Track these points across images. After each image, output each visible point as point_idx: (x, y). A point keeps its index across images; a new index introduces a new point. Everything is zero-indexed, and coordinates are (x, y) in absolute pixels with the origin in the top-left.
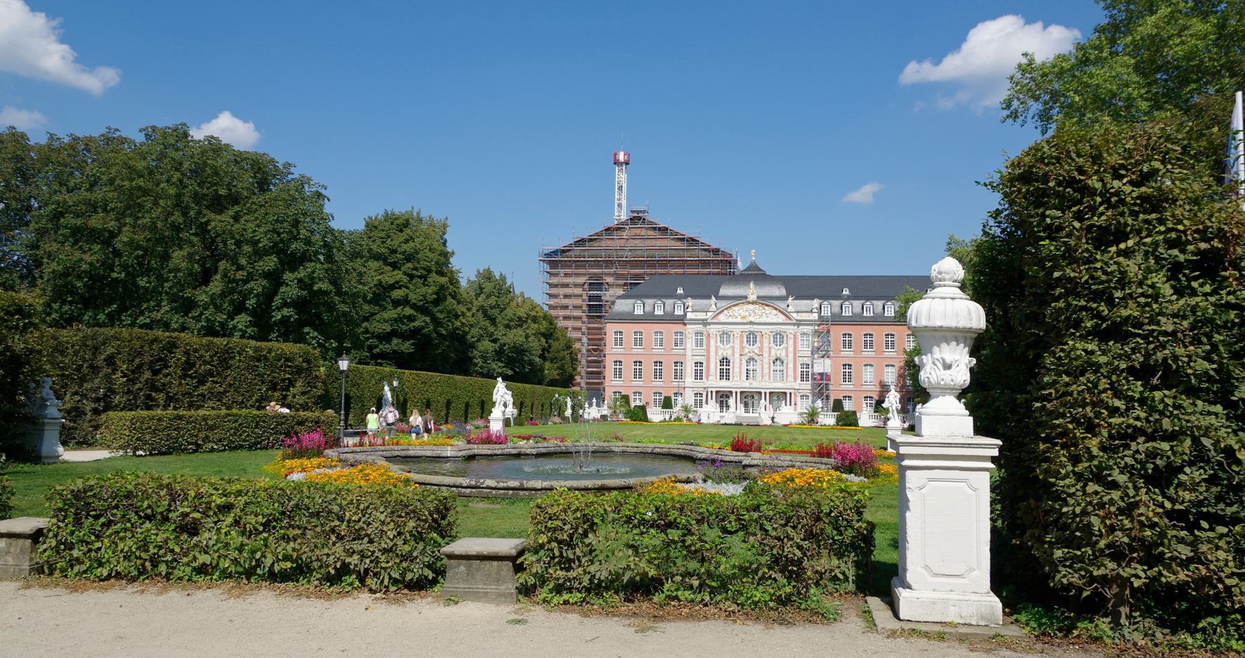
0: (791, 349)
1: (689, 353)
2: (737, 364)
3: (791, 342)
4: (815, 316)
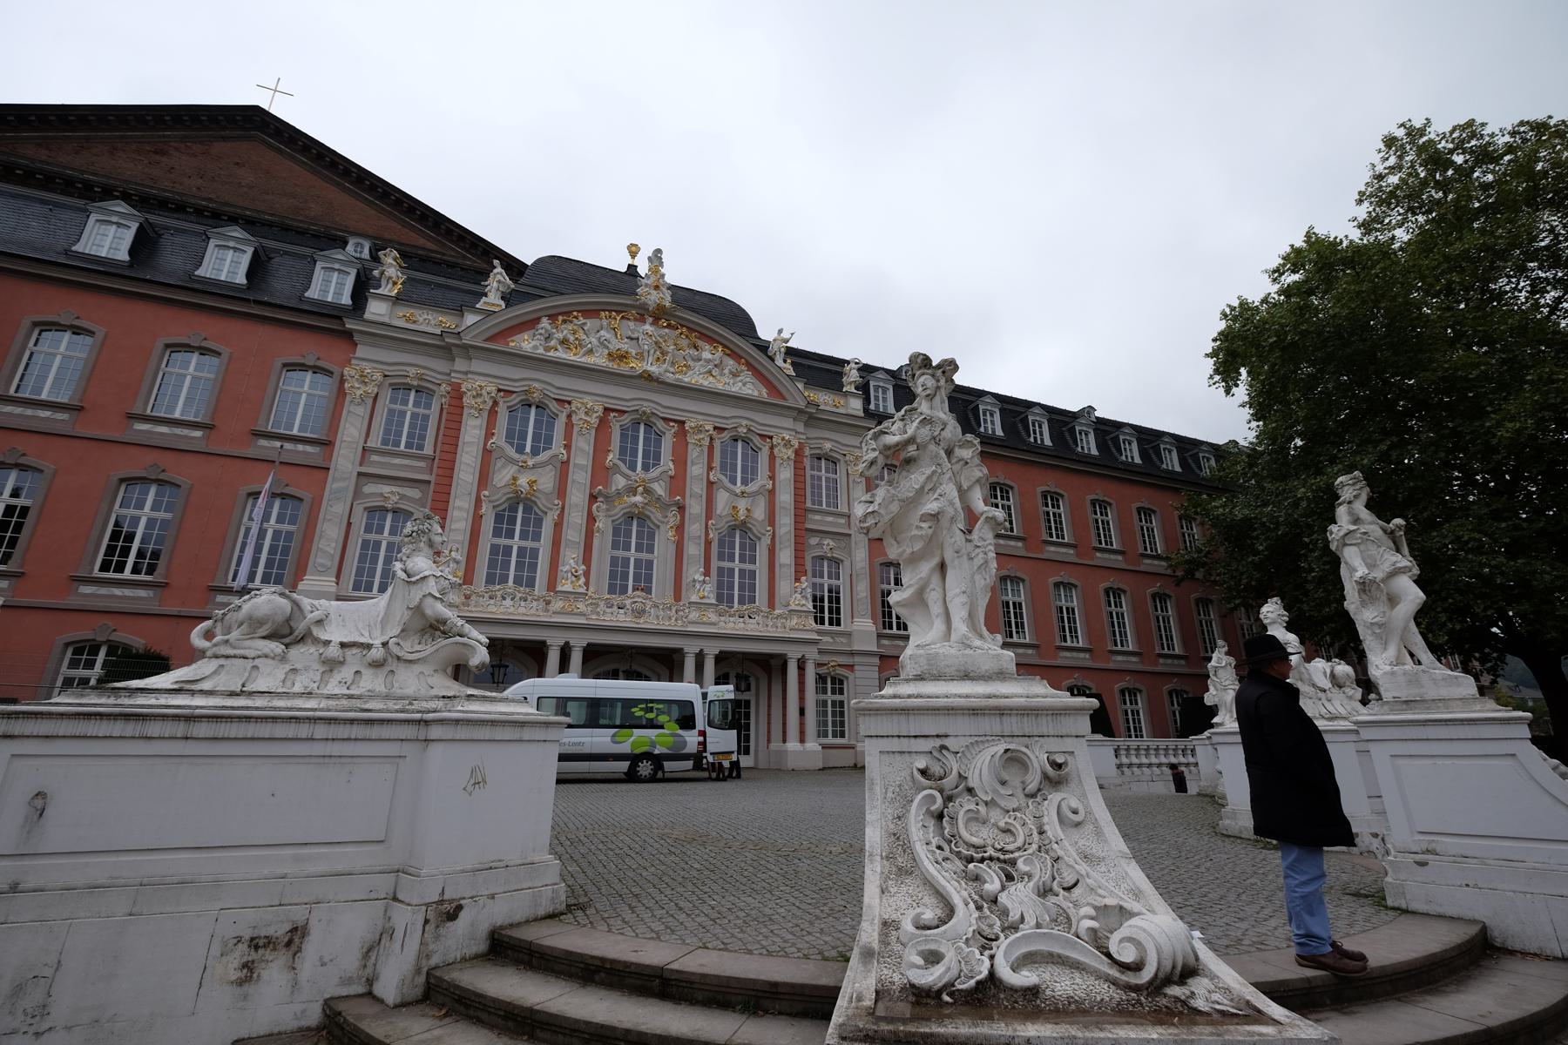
0: (785, 497)
1: (345, 461)
3: (785, 474)
4: (856, 405)
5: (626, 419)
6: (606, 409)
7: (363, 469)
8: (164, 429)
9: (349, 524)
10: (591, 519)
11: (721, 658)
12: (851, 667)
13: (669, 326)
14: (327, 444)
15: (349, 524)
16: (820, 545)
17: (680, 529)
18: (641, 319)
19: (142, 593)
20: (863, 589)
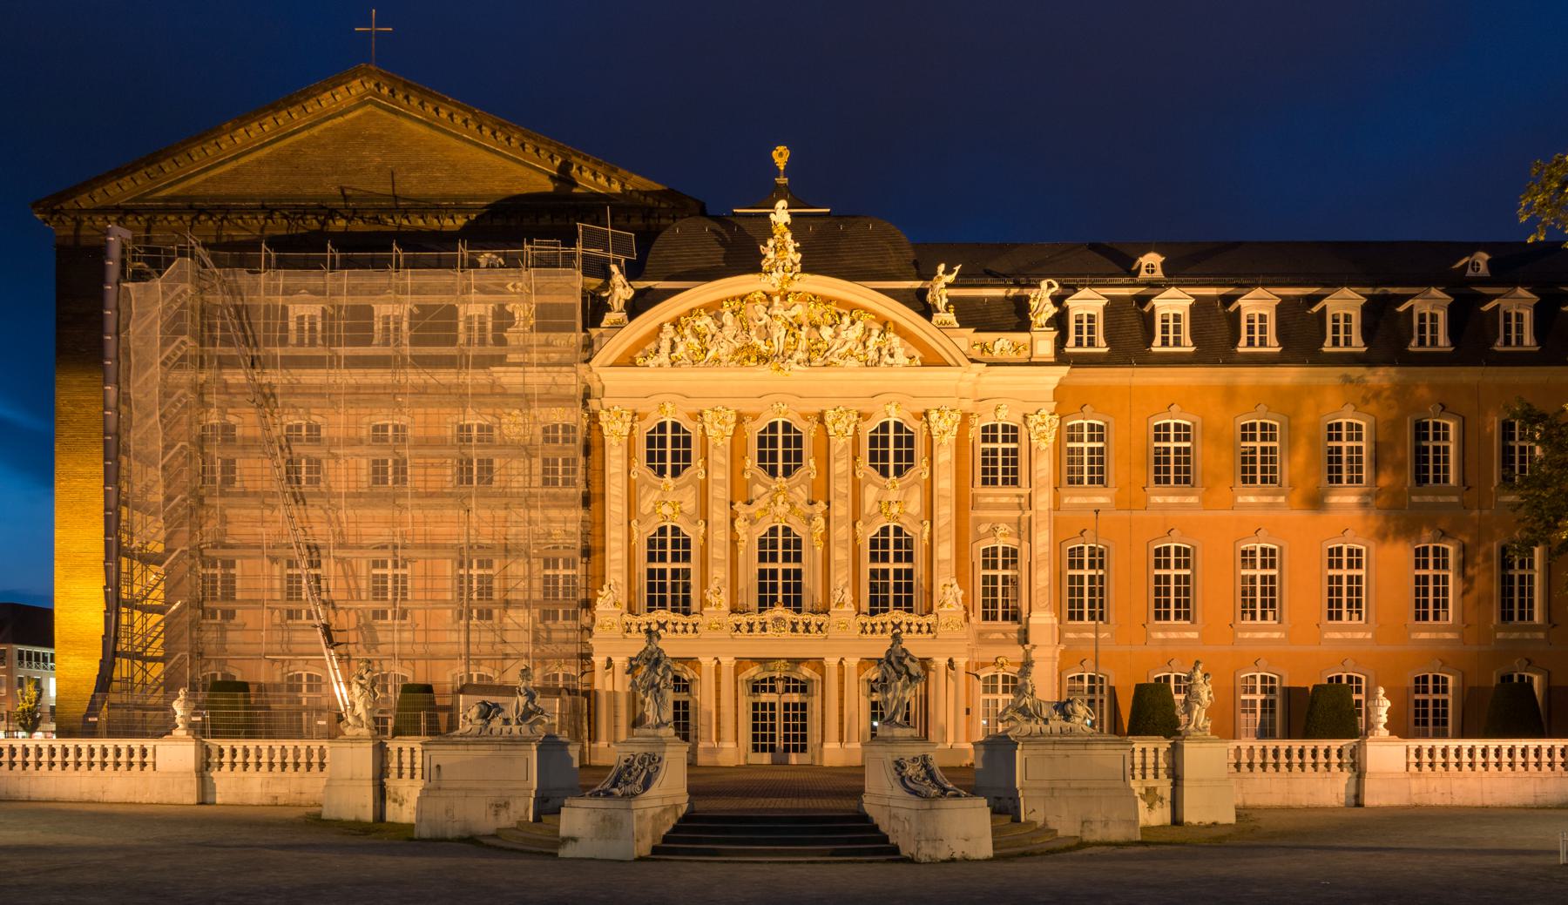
0: (945, 484)
2: (719, 553)
20: (1043, 577)
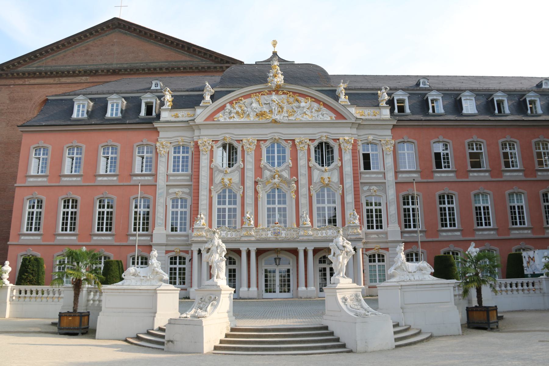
0: (348, 169)
1: (161, 182)
2: (249, 200)
3: (347, 157)
4: (386, 113)
5: (268, 143)
6: (258, 140)
7: (168, 183)
8: (105, 178)
9: (166, 206)
10: (256, 192)
11: (316, 251)
12: (387, 249)
13: (284, 93)
14: (155, 175)
15: (166, 206)
16: (369, 190)
17: (297, 192)
18: (270, 93)
19: (109, 238)
20: (393, 209)
